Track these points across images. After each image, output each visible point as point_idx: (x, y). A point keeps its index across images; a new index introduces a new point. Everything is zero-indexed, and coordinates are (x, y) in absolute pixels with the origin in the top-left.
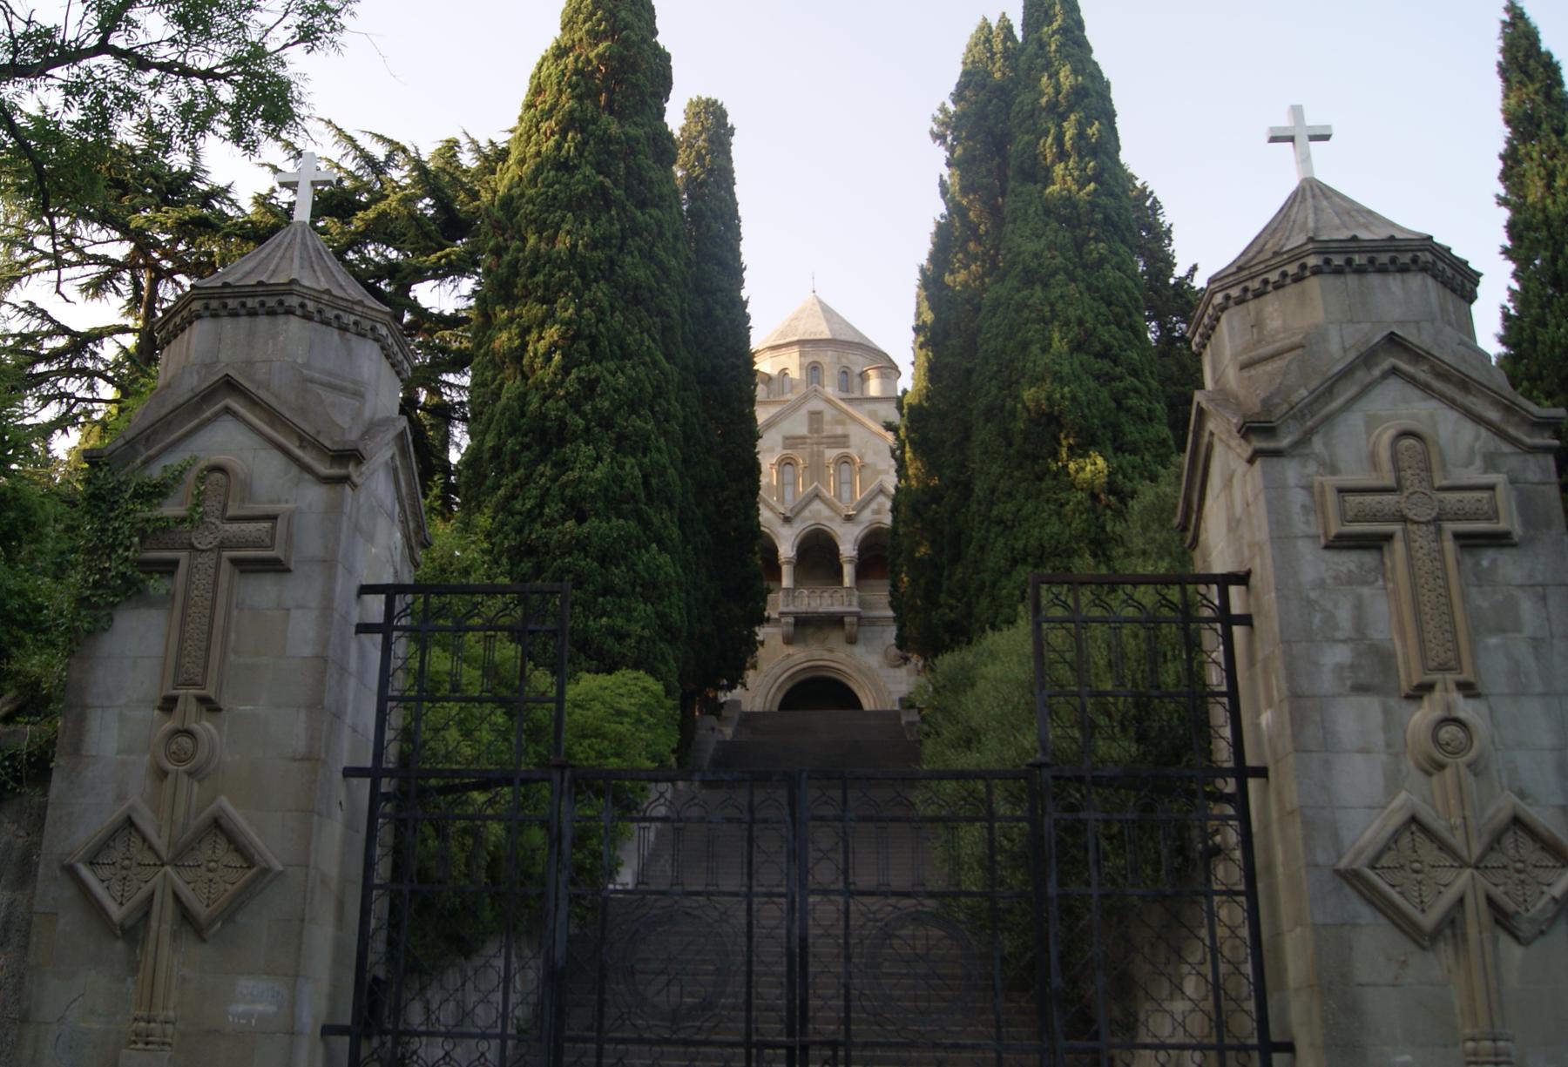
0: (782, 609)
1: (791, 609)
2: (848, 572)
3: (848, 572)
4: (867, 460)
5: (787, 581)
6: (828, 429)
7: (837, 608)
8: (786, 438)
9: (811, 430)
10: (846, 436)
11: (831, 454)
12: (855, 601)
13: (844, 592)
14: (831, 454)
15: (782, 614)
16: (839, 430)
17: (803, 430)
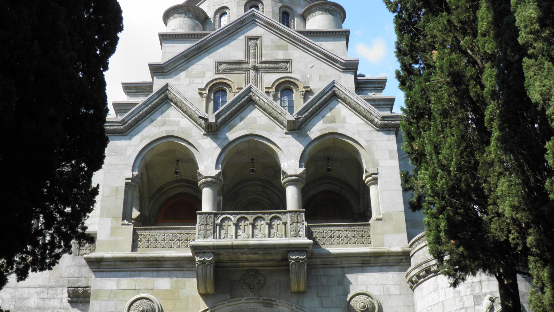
0: (200, 242)
1: (210, 241)
2: (292, 195)
3: (292, 195)
4: (312, 86)
5: (207, 206)
6: (267, 54)
7: (278, 240)
8: (220, 63)
9: (248, 56)
10: (287, 62)
11: (270, 79)
12: (303, 233)
13: (287, 218)
14: (270, 79)
15: (197, 249)
16: (280, 55)
17: (240, 56)
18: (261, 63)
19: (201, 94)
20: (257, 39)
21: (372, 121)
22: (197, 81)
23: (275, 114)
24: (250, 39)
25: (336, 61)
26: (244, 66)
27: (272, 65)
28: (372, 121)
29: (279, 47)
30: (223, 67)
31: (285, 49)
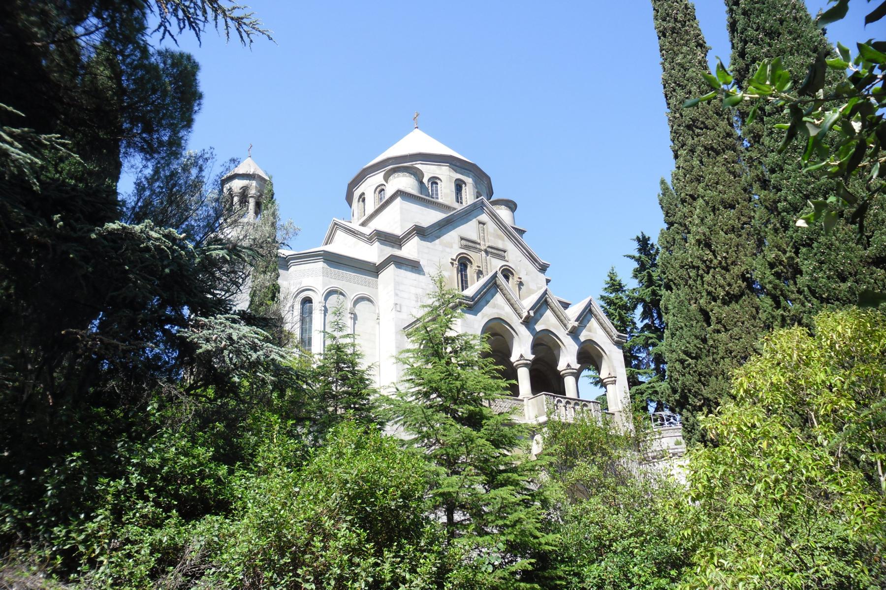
8: (462, 239)
10: (505, 252)
18: (489, 247)
19: (452, 264)
20: (484, 224)
21: (611, 337)
22: (448, 250)
23: (562, 318)
24: (480, 223)
25: (536, 261)
26: (478, 246)
27: (495, 251)
28: (611, 337)
29: (499, 237)
30: (464, 242)
31: (503, 240)
